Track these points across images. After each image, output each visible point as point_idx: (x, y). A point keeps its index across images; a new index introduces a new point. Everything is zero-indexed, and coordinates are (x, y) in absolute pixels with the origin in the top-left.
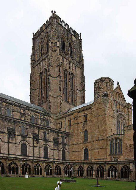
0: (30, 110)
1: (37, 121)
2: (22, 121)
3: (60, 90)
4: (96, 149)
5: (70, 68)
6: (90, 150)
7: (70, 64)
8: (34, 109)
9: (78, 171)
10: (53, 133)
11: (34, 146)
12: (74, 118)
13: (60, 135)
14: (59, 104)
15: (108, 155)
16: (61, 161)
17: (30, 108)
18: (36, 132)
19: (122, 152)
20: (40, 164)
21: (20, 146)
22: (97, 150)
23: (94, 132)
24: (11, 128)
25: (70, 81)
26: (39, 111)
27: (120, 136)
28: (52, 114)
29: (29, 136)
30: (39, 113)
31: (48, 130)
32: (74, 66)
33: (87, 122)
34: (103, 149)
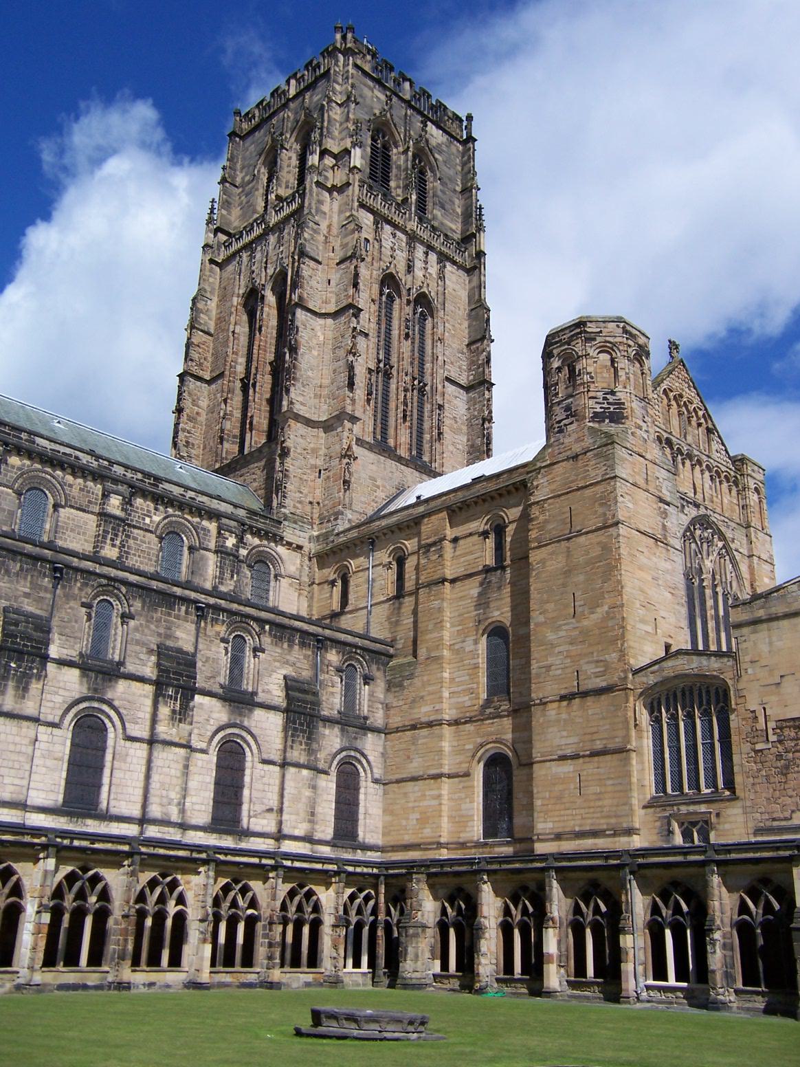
0: (160, 499)
1: (195, 568)
2: (106, 570)
3: (351, 385)
4: (563, 758)
5: (410, 268)
6: (521, 765)
7: (411, 249)
8: (191, 494)
9: (443, 927)
10: (291, 646)
11: (152, 741)
13: (333, 657)
16: (326, 851)
17: (167, 486)
18: (184, 636)
19: (730, 784)
21: (59, 743)
22: (567, 768)
23: (551, 636)
24: (29, 616)
25: (407, 336)
26: (215, 505)
27: (712, 666)
29: (130, 668)
30: (213, 515)
32: (433, 257)
34: (608, 757)
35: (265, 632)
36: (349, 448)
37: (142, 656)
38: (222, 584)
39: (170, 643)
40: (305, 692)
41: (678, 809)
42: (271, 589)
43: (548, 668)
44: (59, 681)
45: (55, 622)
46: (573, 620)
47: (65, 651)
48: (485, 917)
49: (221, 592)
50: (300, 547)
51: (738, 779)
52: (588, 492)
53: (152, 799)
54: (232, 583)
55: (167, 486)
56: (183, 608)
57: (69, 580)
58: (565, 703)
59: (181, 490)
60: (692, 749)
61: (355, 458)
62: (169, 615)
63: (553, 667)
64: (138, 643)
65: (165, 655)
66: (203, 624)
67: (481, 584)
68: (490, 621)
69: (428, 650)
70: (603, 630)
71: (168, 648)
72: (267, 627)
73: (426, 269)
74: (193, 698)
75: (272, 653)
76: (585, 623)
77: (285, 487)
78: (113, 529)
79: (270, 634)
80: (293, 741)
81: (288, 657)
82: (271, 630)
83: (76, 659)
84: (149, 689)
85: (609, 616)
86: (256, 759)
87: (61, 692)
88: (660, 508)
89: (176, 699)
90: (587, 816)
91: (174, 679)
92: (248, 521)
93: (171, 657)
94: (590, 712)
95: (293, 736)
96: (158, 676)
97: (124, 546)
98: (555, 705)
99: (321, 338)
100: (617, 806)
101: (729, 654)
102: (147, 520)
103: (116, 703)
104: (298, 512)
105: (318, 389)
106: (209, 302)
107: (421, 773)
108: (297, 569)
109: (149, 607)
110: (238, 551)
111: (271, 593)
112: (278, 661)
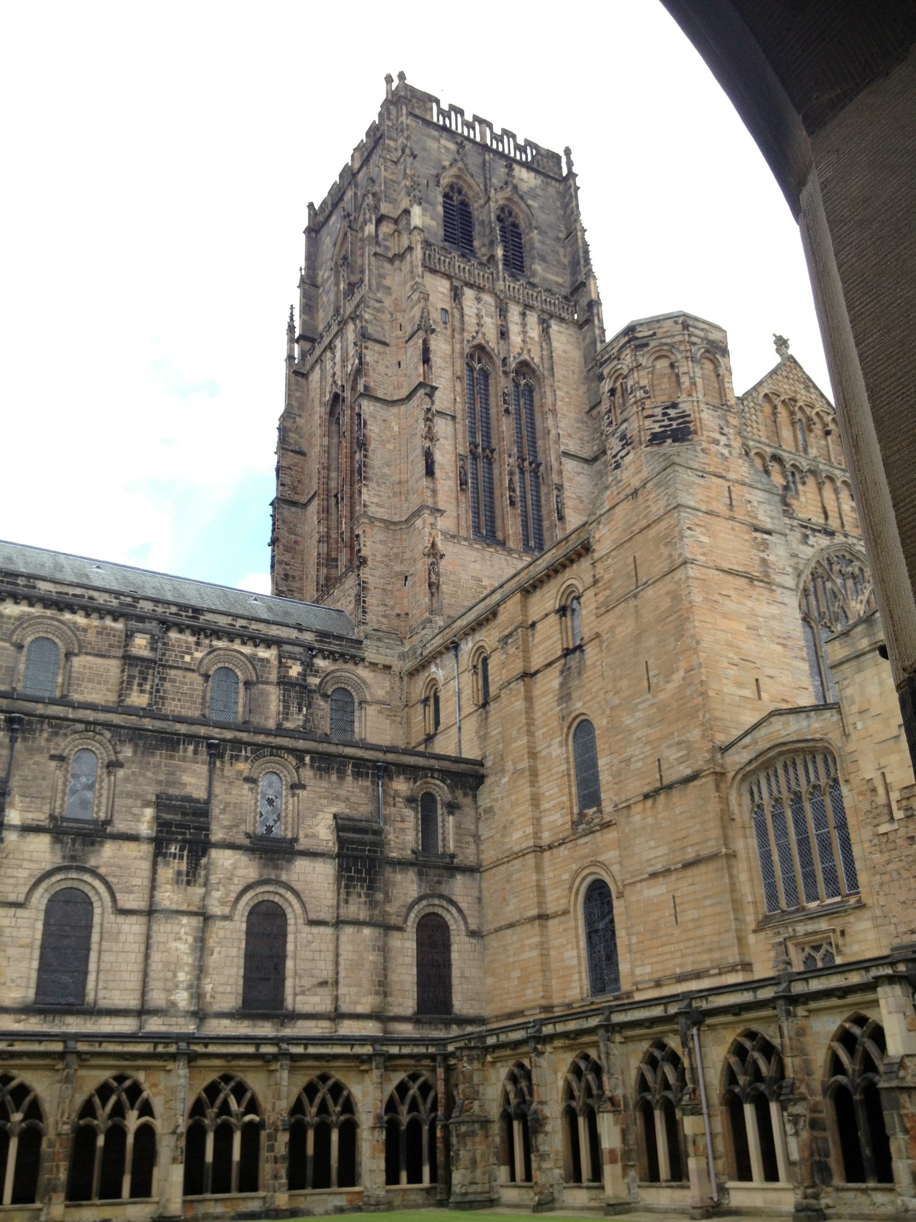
4: (654, 875)
5: (503, 334)
7: (503, 312)
8: (241, 622)
12: (504, 640)
14: (421, 566)
15: (751, 920)
20: (141, 1076)
25: (507, 411)
26: (274, 631)
28: (379, 635)
29: (120, 825)
31: (299, 754)
32: (532, 319)
33: (580, 648)
34: (702, 868)
35: (305, 765)
36: (433, 545)
37: (136, 811)
38: (287, 719)
39: (172, 791)
40: (363, 831)
41: (794, 930)
42: (356, 719)
43: (628, 761)
44: (23, 852)
45: (15, 783)
46: (649, 696)
47: (30, 816)
48: (542, 1103)
49: (285, 729)
50: (387, 668)
51: (863, 878)
52: (652, 533)
53: (152, 984)
54: (301, 717)
55: (209, 617)
56: (191, 748)
57: (32, 731)
58: (649, 803)
59: (229, 620)
60: (803, 842)
61: (442, 556)
62: (172, 757)
63: (633, 760)
64: (129, 795)
65: (165, 805)
66: (218, 764)
67: (562, 672)
68: (573, 715)
69: (514, 763)
70: (681, 702)
71: (170, 798)
72: (307, 759)
73: (524, 333)
74: (204, 852)
75: (318, 789)
76: (662, 696)
77: (364, 602)
78: (141, 672)
79: (312, 766)
80: (348, 894)
81: (339, 792)
82: (312, 760)
83: (46, 823)
84: (146, 849)
85: (687, 682)
86: (301, 921)
87: (26, 865)
88: (756, 538)
89: (181, 857)
90: (687, 951)
91: (177, 833)
92: (316, 645)
93: (175, 806)
94: (677, 811)
95: (347, 886)
96: (158, 832)
97: (158, 691)
98: (639, 807)
99: (396, 429)
100: (720, 933)
101: (836, 707)
102: (187, 658)
103: (102, 871)
104: (383, 627)
105: (396, 486)
106: (298, 419)
107: (518, 917)
108: (387, 693)
109: (143, 753)
110: (305, 680)
111: (357, 724)
112: (325, 798)
